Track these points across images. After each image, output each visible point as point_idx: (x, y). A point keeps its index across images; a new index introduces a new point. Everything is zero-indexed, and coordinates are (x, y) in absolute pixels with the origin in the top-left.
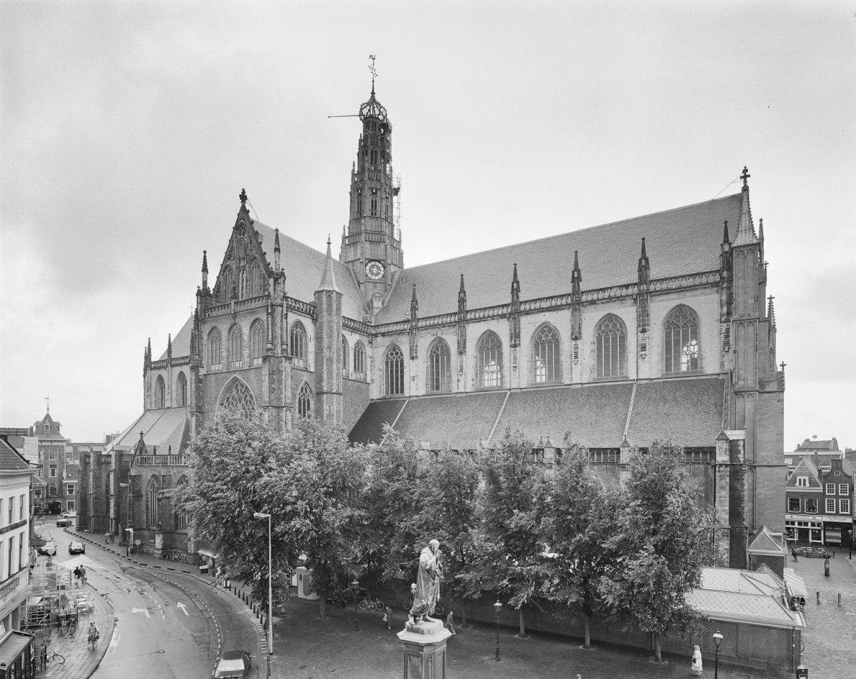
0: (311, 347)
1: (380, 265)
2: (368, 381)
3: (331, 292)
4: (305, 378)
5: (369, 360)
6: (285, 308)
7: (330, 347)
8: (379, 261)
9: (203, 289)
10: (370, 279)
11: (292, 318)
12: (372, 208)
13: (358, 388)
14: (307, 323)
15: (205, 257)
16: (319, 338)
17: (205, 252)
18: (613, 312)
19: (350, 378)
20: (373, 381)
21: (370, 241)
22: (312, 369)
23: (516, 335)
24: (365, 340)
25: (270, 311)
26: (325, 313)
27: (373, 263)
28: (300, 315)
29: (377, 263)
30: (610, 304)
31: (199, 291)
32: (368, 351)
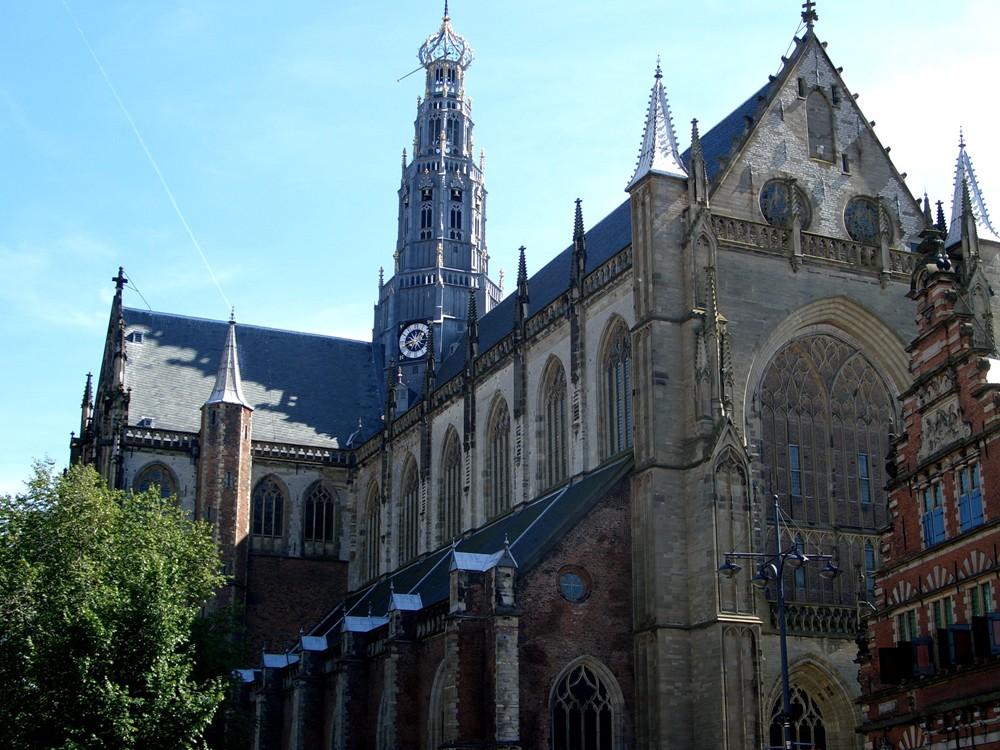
2: (343, 557)
7: (210, 500)
8: (425, 323)
9: (82, 434)
12: (423, 226)
15: (88, 383)
16: (198, 488)
17: (89, 376)
18: (555, 351)
19: (291, 553)
20: (353, 555)
23: (469, 427)
24: (336, 477)
25: (94, 455)
26: (206, 444)
27: (412, 327)
28: (161, 454)
29: (421, 326)
30: (552, 336)
31: (72, 438)
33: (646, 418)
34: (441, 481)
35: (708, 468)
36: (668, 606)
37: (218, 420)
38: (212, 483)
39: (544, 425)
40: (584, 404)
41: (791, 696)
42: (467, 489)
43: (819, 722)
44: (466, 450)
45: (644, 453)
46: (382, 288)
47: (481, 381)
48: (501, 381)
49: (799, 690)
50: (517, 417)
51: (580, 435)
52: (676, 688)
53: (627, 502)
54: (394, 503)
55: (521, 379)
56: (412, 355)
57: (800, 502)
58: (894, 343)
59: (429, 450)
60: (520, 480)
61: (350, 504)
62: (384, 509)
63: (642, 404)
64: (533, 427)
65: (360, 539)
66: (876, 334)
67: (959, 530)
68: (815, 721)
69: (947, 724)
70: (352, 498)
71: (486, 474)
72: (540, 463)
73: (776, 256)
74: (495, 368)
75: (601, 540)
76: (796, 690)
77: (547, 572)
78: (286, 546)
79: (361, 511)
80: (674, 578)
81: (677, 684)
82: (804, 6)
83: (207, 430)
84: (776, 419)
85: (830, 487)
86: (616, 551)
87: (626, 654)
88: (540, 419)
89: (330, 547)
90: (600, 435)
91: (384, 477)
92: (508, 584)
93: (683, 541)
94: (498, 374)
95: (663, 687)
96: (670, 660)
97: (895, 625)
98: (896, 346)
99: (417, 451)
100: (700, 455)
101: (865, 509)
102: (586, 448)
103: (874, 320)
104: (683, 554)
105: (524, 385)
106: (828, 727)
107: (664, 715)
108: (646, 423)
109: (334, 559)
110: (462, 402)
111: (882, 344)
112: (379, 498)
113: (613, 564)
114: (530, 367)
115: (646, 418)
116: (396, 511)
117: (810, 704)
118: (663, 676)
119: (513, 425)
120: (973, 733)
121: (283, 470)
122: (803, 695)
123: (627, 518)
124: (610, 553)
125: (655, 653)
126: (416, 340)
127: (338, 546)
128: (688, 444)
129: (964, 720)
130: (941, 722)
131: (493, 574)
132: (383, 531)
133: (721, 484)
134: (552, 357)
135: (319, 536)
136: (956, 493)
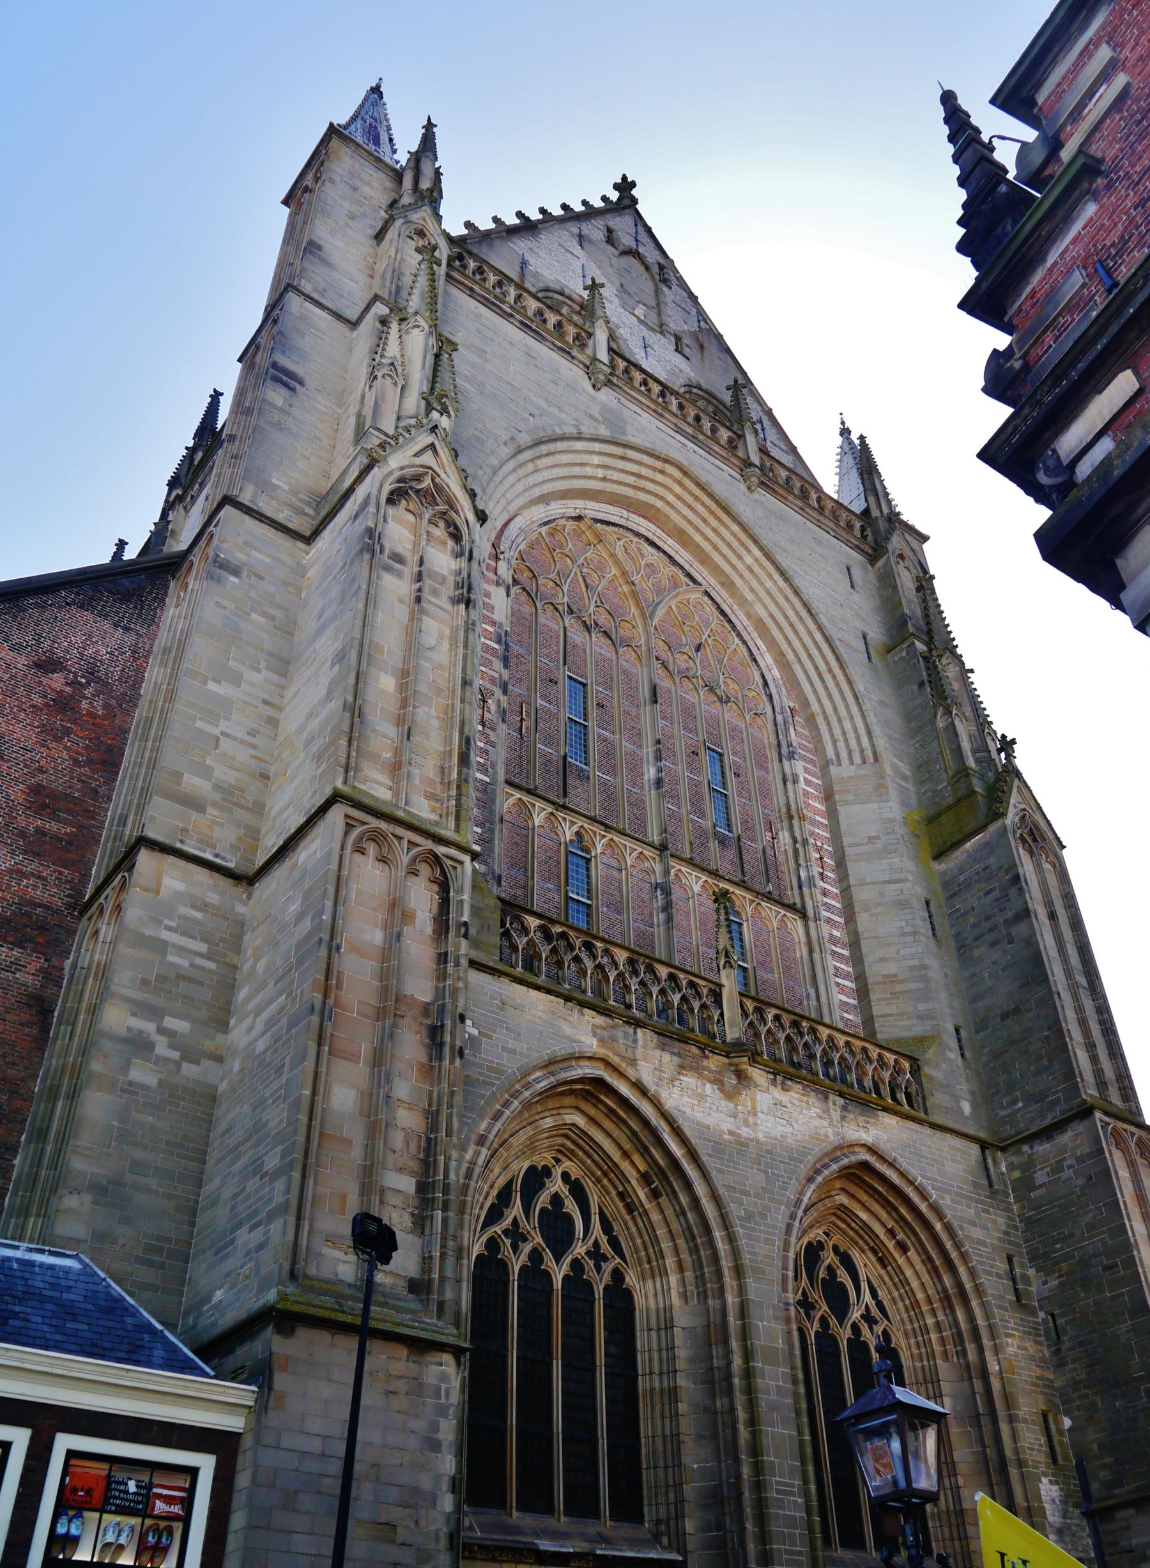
36: (194, 804)
41: (542, 1186)
43: (618, 1275)
49: (565, 1176)
52: (162, 1031)
58: (770, 577)
66: (740, 557)
68: (608, 1268)
73: (560, 349)
76: (558, 1172)
80: (224, 743)
81: (170, 1022)
82: (616, 187)
84: (541, 619)
85: (651, 773)
86: (84, 704)
87: (36, 963)
93: (275, 678)
95: (116, 1018)
96: (162, 947)
98: (775, 582)
103: (735, 528)
104: (266, 702)
106: (646, 1296)
107: (96, 1106)
111: (747, 575)
113: (67, 732)
117: (595, 1219)
118: (123, 981)
122: (577, 1190)
124: (63, 704)
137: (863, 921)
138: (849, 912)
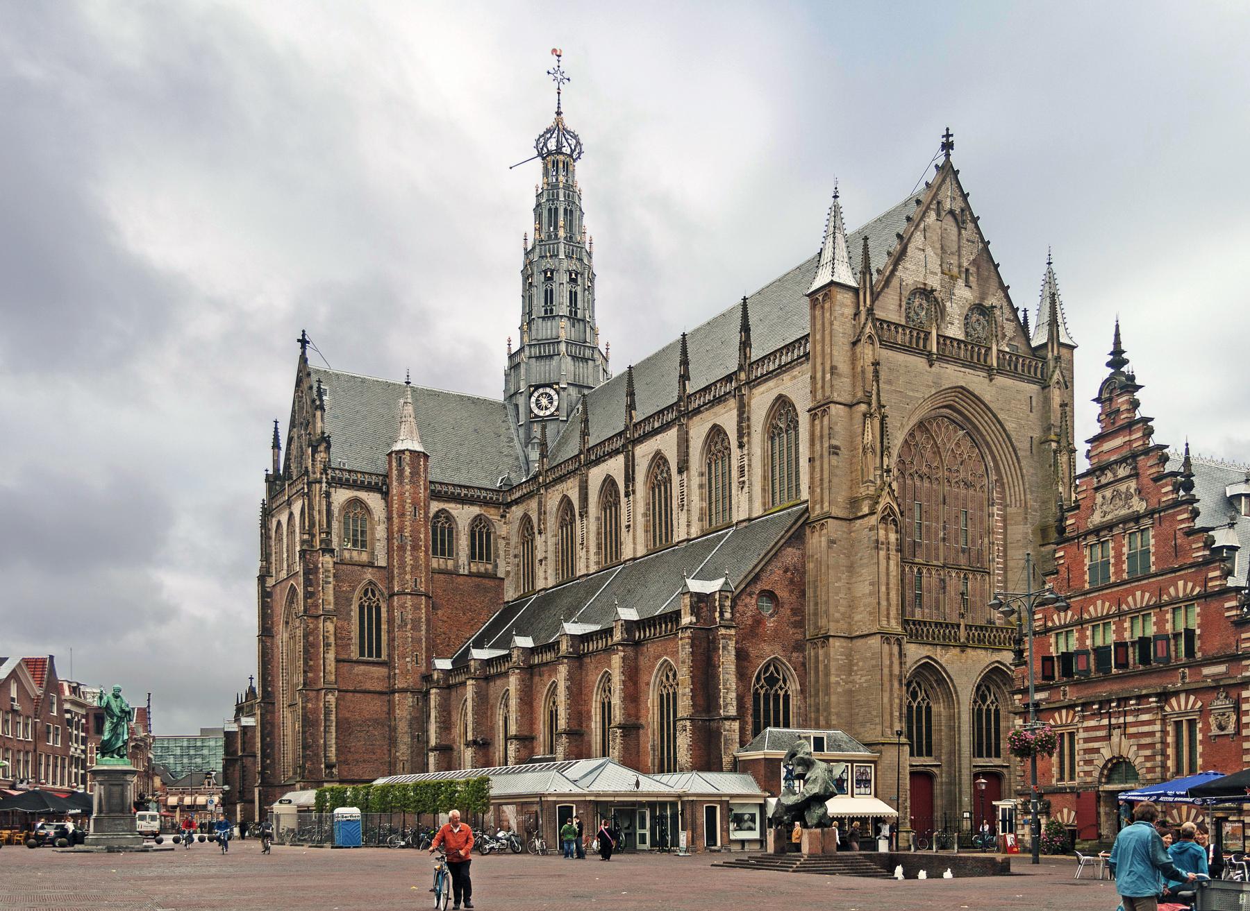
0: (380, 532)
1: (552, 392)
2: (501, 574)
3: (403, 452)
4: (369, 576)
5: (501, 543)
6: (324, 485)
7: (401, 530)
8: (550, 386)
10: (537, 416)
11: (341, 496)
13: (478, 586)
14: (374, 501)
16: (389, 519)
19: (461, 571)
20: (508, 573)
21: (537, 358)
22: (382, 562)
23: (630, 478)
24: (493, 514)
26: (395, 483)
27: (541, 391)
29: (548, 390)
32: (501, 529)
33: (822, 480)
34: (598, 519)
35: (873, 520)
37: (404, 464)
38: (402, 515)
39: (705, 479)
40: (749, 465)
42: (629, 526)
44: (627, 495)
45: (818, 507)
46: (511, 357)
47: (641, 442)
48: (667, 442)
50: (680, 472)
51: (746, 489)
53: (803, 543)
54: (549, 535)
55: (684, 443)
56: (541, 414)
57: (920, 545)
59: (586, 494)
60: (683, 521)
61: (504, 533)
62: (539, 540)
63: (818, 469)
64: (696, 482)
65: (511, 559)
67: (1125, 576)
69: (1100, 708)
70: (506, 528)
71: (645, 515)
72: (701, 509)
74: (656, 432)
75: (785, 572)
77: (750, 595)
78: (457, 566)
79: (514, 540)
83: (395, 472)
85: (941, 535)
88: (702, 474)
89: (489, 567)
90: (764, 490)
91: (540, 514)
92: (728, 603)
94: (659, 437)
97: (1052, 640)
99: (574, 496)
100: (866, 510)
101: (963, 551)
102: (750, 500)
105: (687, 447)
108: (822, 484)
109: (493, 576)
110: (621, 459)
112: (527, 529)
114: (691, 433)
115: (822, 480)
116: (551, 541)
119: (676, 479)
120: (1125, 714)
121: (453, 505)
123: (803, 555)
124: (792, 581)
125: (827, 655)
126: (544, 401)
127: (496, 566)
128: (854, 502)
129: (1118, 706)
130: (1096, 707)
131: (717, 596)
132: (539, 555)
133: (882, 532)
134: (715, 426)
135: (481, 558)
136: (1125, 550)
137: (1010, 574)
138: (1005, 569)
